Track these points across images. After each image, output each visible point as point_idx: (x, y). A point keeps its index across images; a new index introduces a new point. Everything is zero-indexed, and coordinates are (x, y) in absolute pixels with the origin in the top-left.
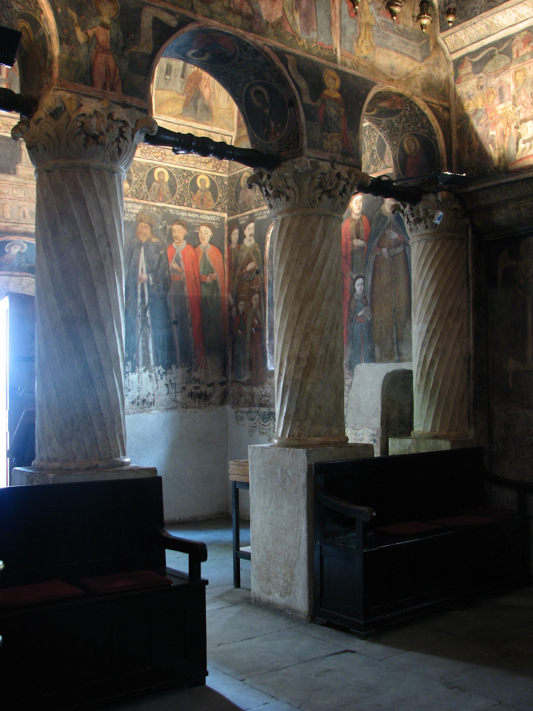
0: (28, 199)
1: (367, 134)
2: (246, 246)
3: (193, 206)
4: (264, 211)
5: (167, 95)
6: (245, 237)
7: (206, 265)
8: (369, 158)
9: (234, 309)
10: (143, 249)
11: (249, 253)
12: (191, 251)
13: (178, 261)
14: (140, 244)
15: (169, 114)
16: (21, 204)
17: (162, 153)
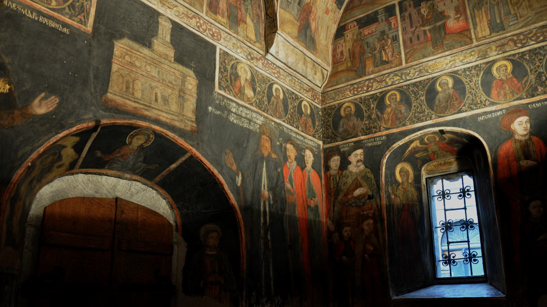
0: (161, 81)
1: (528, 58)
2: (351, 172)
3: (300, 128)
4: (376, 137)
5: (287, 16)
6: (350, 163)
7: (311, 189)
8: (534, 80)
9: (337, 234)
10: (265, 164)
11: (357, 178)
12: (300, 173)
13: (291, 182)
14: (262, 158)
15: (289, 34)
16: (154, 84)
17: (278, 72)
